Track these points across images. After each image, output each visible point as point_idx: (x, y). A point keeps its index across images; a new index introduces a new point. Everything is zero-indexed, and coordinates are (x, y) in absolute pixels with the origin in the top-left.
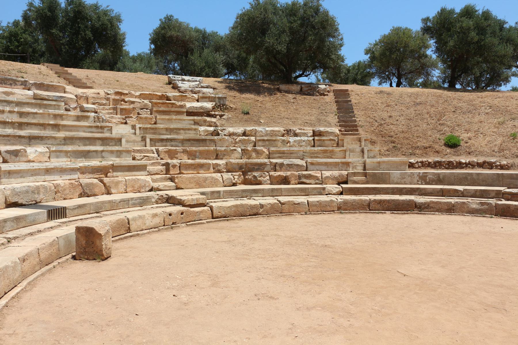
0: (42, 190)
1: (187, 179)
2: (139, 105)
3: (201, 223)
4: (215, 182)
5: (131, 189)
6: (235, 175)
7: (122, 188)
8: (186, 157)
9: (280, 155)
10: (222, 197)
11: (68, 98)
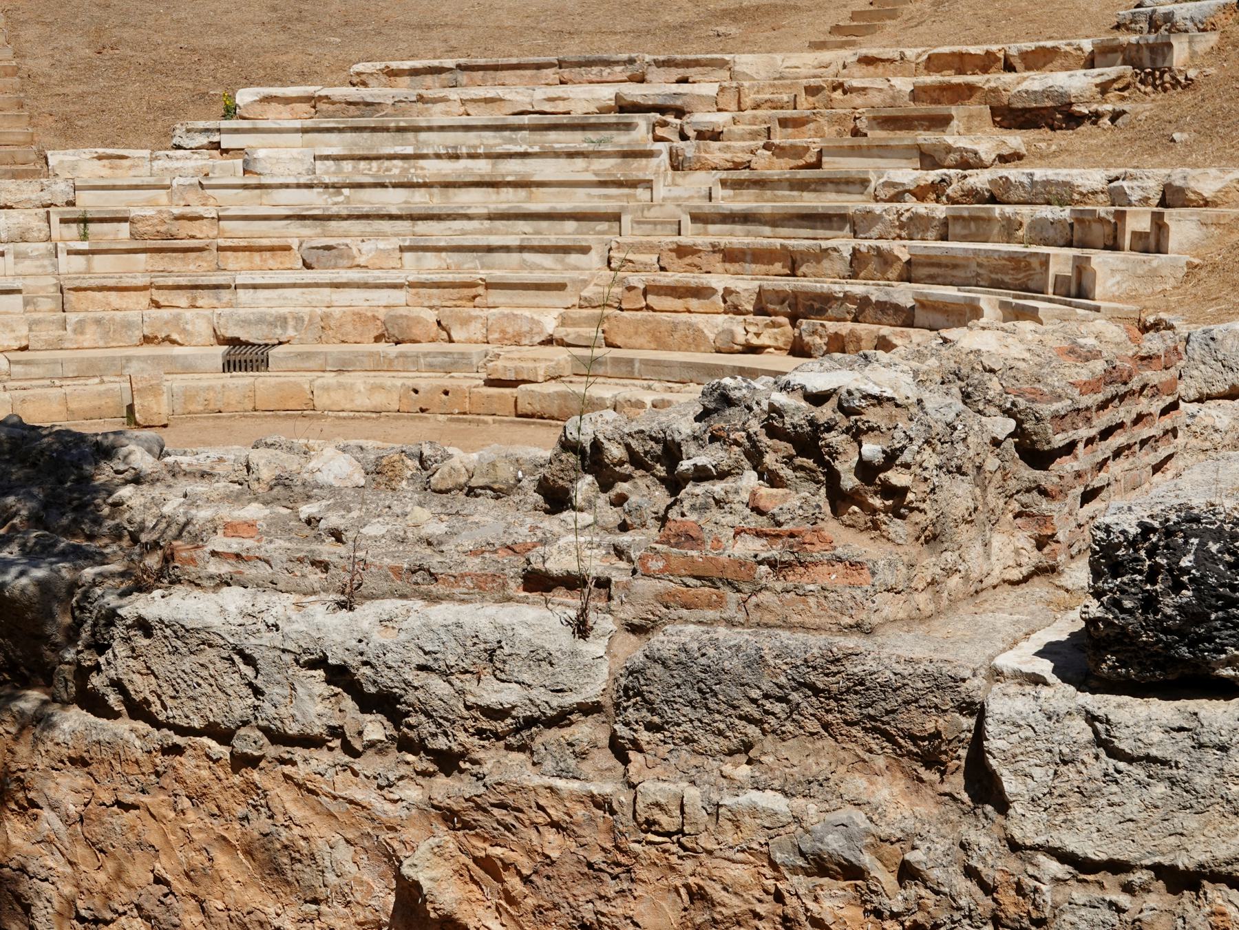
0: (291, 323)
1: (629, 322)
2: (876, 99)
3: (465, 421)
4: (695, 339)
5: (496, 336)
6: (750, 324)
7: (476, 330)
9: (934, 271)
10: (636, 375)
11: (693, 96)
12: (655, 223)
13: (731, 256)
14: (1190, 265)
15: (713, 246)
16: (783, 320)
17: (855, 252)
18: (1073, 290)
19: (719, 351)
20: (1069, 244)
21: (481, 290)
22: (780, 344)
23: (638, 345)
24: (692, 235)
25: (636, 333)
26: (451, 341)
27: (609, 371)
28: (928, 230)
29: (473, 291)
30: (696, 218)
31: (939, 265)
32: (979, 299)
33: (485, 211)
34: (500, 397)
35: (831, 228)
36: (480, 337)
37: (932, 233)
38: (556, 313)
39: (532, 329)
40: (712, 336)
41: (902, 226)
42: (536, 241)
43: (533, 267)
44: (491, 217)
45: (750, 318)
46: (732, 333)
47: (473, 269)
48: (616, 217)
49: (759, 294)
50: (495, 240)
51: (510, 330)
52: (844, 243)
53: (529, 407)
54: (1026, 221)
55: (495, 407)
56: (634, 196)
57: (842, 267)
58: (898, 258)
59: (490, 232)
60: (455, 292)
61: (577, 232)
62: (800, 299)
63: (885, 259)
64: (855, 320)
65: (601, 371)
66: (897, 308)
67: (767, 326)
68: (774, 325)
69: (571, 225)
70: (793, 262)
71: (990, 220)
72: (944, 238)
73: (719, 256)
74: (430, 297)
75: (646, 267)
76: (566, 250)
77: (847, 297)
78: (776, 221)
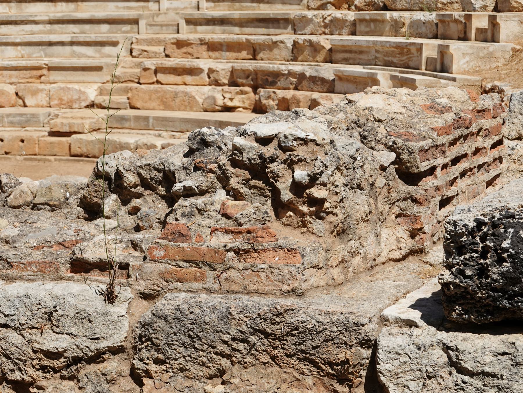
1: (145, 92)
3: (36, 160)
4: (190, 103)
5: (56, 102)
6: (226, 92)
8: (205, 54)
10: (151, 127)
12: (162, 26)
13: (213, 47)
14: (513, 49)
15: (201, 40)
16: (248, 89)
17: (295, 44)
18: (438, 67)
19: (206, 111)
20: (436, 37)
21: (45, 72)
22: (246, 105)
23: (151, 107)
24: (186, 33)
25: (150, 99)
26: (25, 106)
27: (133, 124)
28: (343, 28)
29: (40, 72)
30: (189, 22)
31: (350, 52)
32: (376, 74)
33: (47, 18)
34: (59, 143)
35: (279, 28)
36: (45, 103)
37: (345, 31)
38: (96, 86)
39: (80, 98)
40: (200, 101)
41: (326, 26)
42: (82, 38)
43: (80, 56)
44: (51, 22)
45: (226, 88)
46: (214, 98)
47: (40, 57)
48: (136, 22)
49: (232, 72)
50: (54, 38)
51: (65, 98)
52: (287, 38)
53: (79, 150)
54: (407, 22)
55: (56, 150)
56: (147, 7)
57: (286, 54)
58: (323, 47)
59: (50, 32)
60: (28, 73)
61: (109, 32)
62: (259, 76)
63: (315, 48)
64: (296, 89)
65: (127, 125)
66: (323, 80)
67: (237, 93)
68: (242, 93)
69: (105, 27)
70: (254, 51)
71: (383, 21)
72: (354, 33)
73: (205, 47)
74: (10, 77)
75: (156, 55)
76: (102, 44)
77: (291, 74)
78: (242, 23)
